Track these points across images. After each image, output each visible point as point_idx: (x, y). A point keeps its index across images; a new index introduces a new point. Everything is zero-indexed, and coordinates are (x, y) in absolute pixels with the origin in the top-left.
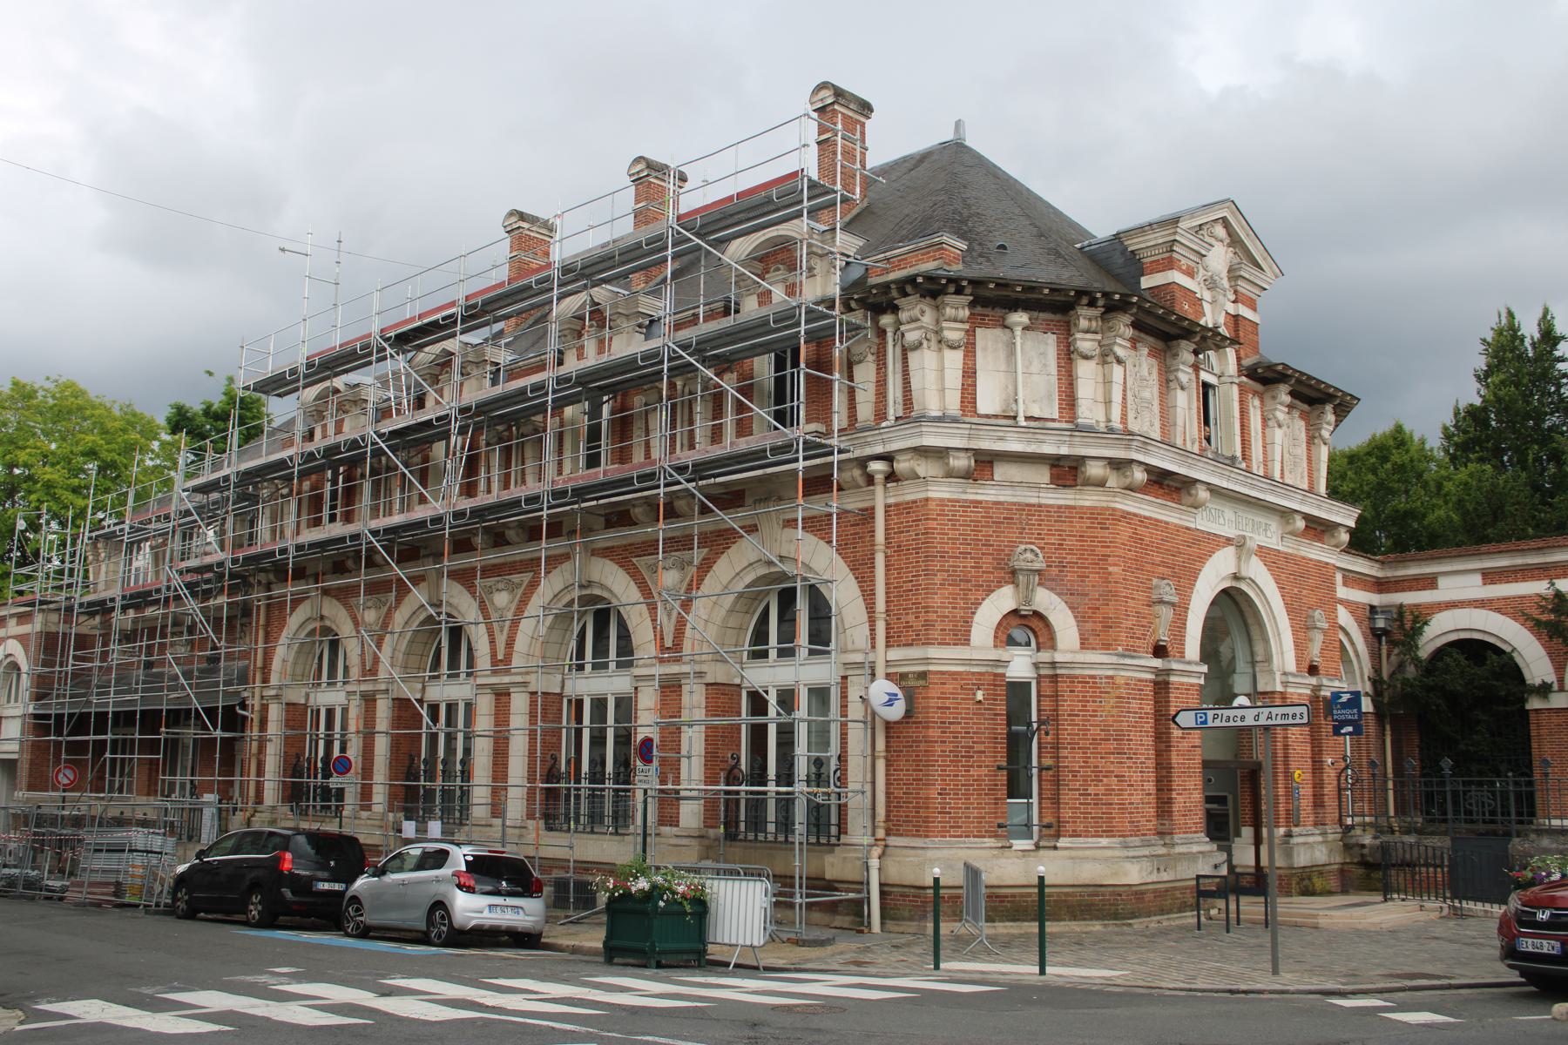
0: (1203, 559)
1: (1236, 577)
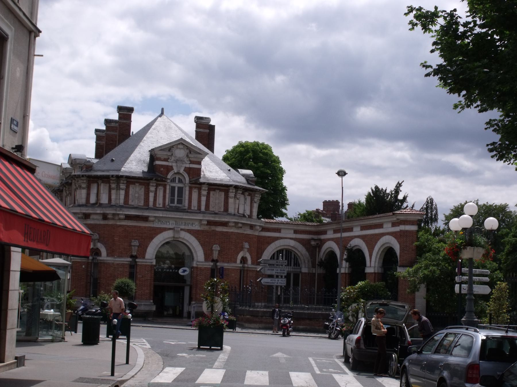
0: (156, 234)
1: (174, 237)
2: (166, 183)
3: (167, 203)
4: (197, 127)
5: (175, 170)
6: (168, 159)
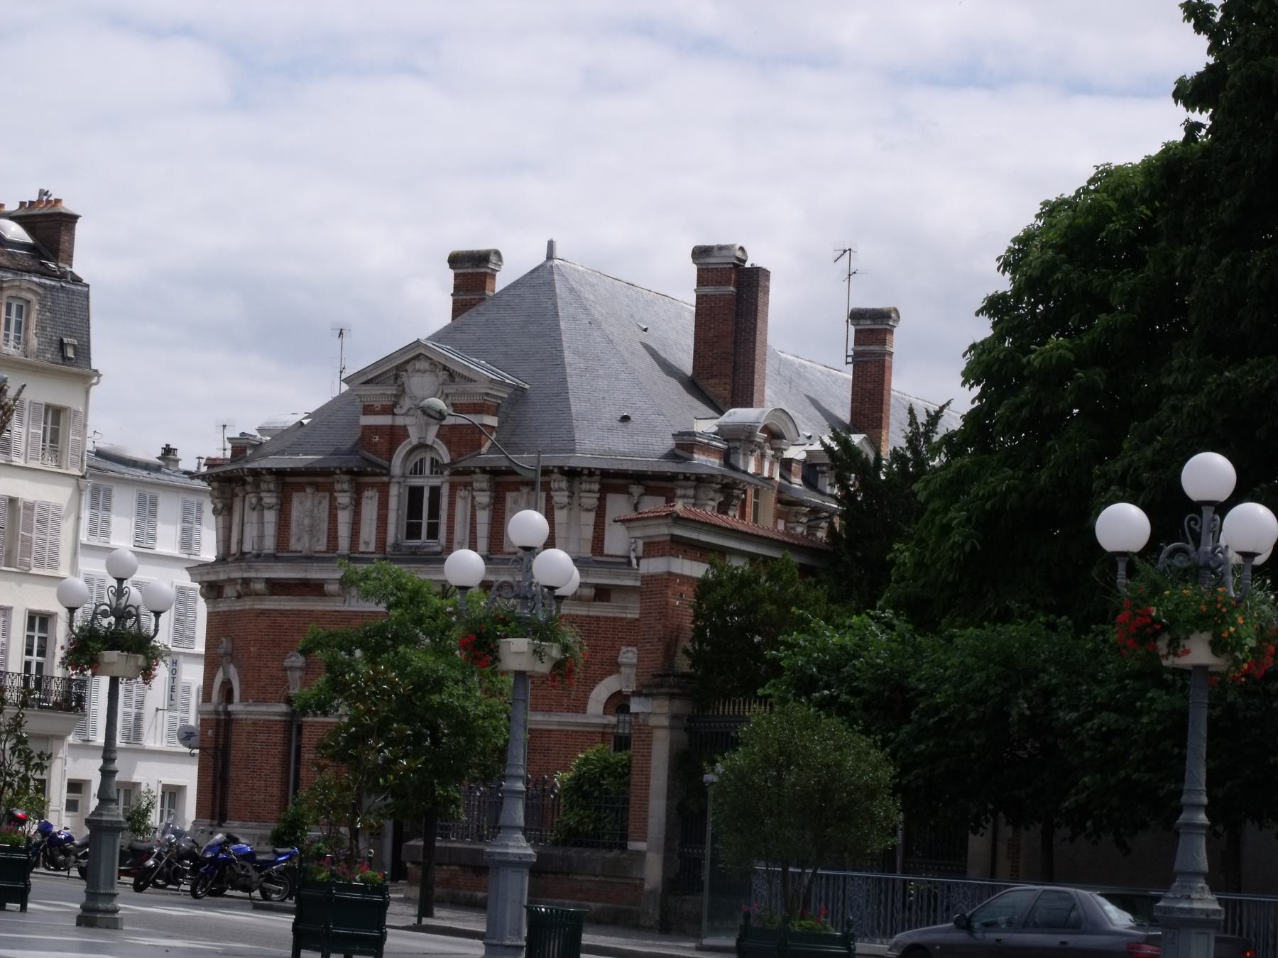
2: (385, 479)
3: (391, 539)
4: (702, 280)
5: (414, 439)
6: (394, 405)
